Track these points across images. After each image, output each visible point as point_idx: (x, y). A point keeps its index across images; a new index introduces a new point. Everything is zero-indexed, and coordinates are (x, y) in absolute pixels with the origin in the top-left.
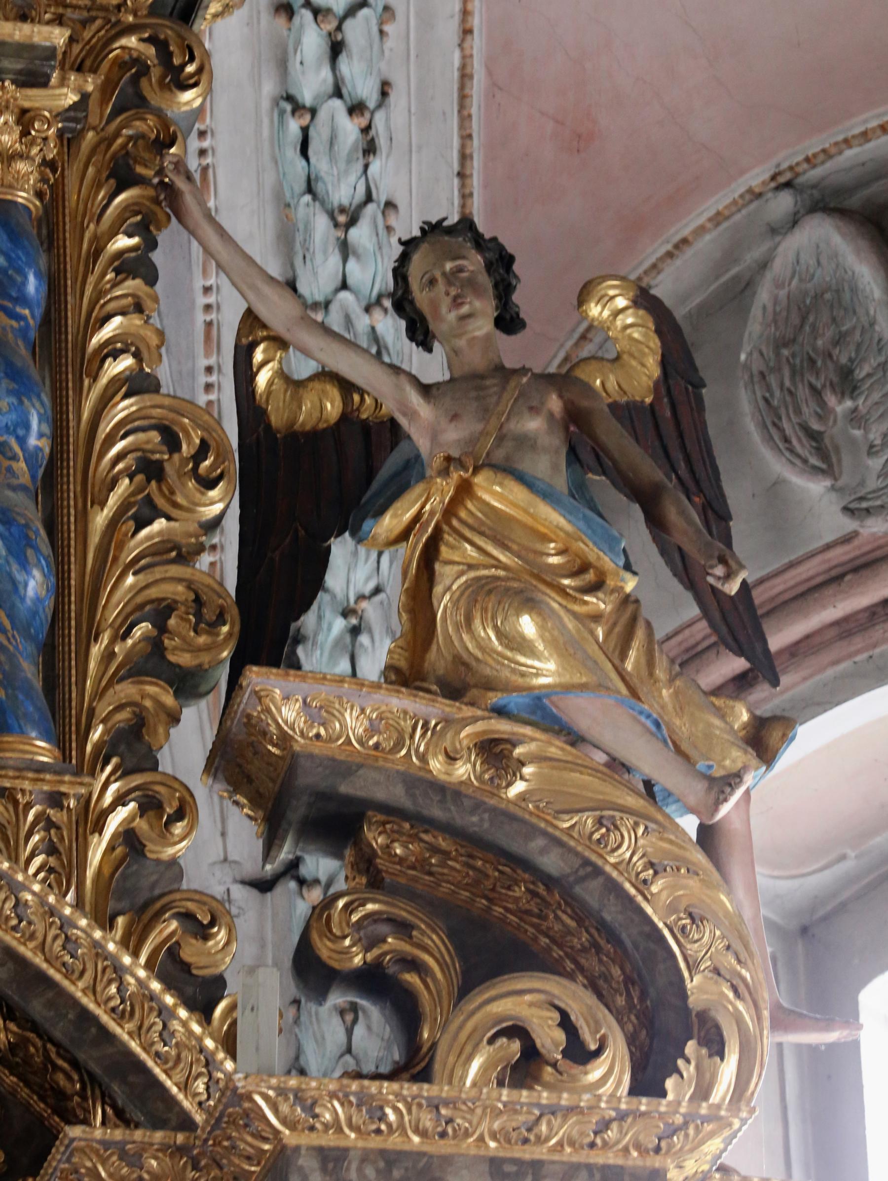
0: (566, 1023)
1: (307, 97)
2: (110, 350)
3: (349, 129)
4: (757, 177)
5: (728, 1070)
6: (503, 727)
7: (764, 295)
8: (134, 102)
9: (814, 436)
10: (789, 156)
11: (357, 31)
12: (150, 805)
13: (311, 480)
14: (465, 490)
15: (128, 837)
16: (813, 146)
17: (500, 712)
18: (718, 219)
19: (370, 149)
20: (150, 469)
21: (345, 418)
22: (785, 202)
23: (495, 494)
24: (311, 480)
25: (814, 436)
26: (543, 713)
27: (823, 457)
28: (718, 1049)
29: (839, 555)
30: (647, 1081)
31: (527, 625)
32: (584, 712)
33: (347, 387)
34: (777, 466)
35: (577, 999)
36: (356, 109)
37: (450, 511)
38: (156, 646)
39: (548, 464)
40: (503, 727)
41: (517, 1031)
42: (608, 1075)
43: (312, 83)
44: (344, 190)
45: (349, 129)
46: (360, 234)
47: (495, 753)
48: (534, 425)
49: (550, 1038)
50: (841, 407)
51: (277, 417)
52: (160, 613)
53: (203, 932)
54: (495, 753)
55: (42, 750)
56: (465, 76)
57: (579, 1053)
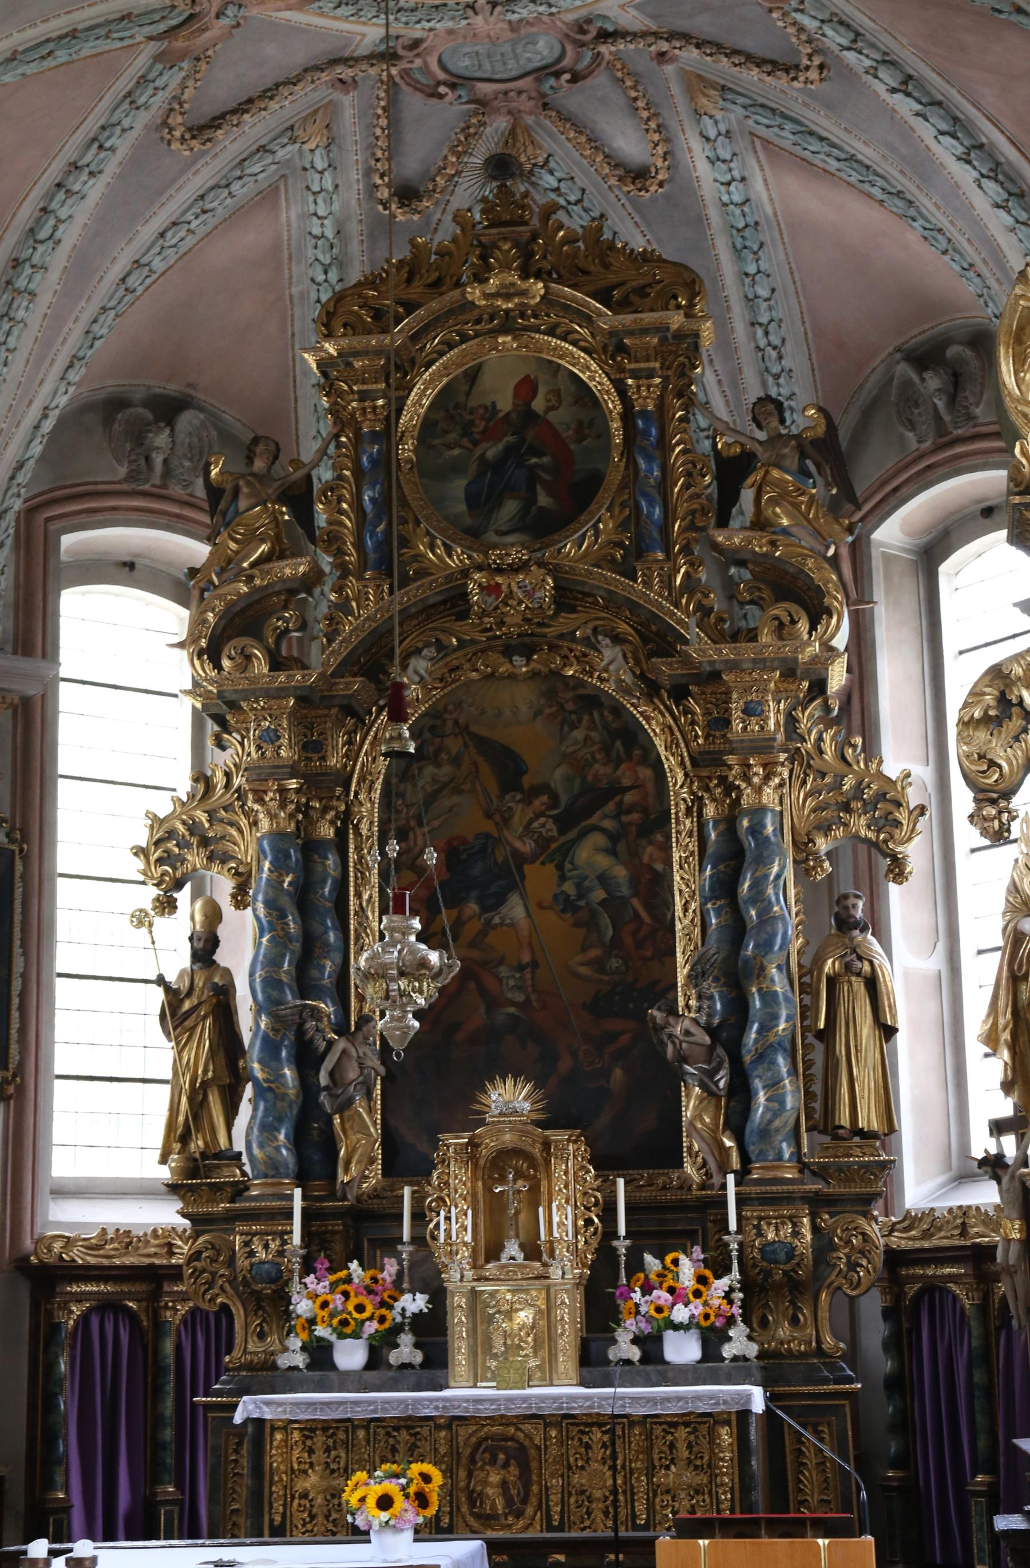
0: (790, 615)
1: (762, 346)
2: (678, 444)
3: (774, 354)
4: (891, 349)
5: (834, 620)
6: (774, 537)
7: (895, 382)
8: (682, 375)
9: (910, 420)
10: (898, 342)
11: (772, 327)
12: (691, 564)
13: (733, 470)
14: (767, 472)
15: (687, 573)
16: (903, 339)
17: (774, 533)
18: (882, 361)
19: (780, 357)
20: (689, 474)
21: (743, 451)
22: (898, 356)
23: (775, 473)
24: (733, 470)
25: (910, 420)
26: (785, 531)
27: (912, 426)
28: (831, 617)
29: (916, 454)
30: (813, 628)
31: (778, 510)
32: (794, 530)
33: (742, 445)
34: (901, 429)
35: (793, 608)
36: (775, 348)
37: (764, 478)
38: (692, 522)
39: (792, 461)
40: (774, 537)
41: (777, 618)
42: (803, 626)
43: (762, 343)
44: (776, 369)
45: (774, 354)
46: (781, 381)
47: (773, 544)
48: (786, 451)
49: (786, 619)
50: (916, 411)
51: (725, 454)
52: (693, 512)
53: (707, 596)
54: (773, 544)
55: (660, 556)
56: (806, 334)
57: (794, 622)
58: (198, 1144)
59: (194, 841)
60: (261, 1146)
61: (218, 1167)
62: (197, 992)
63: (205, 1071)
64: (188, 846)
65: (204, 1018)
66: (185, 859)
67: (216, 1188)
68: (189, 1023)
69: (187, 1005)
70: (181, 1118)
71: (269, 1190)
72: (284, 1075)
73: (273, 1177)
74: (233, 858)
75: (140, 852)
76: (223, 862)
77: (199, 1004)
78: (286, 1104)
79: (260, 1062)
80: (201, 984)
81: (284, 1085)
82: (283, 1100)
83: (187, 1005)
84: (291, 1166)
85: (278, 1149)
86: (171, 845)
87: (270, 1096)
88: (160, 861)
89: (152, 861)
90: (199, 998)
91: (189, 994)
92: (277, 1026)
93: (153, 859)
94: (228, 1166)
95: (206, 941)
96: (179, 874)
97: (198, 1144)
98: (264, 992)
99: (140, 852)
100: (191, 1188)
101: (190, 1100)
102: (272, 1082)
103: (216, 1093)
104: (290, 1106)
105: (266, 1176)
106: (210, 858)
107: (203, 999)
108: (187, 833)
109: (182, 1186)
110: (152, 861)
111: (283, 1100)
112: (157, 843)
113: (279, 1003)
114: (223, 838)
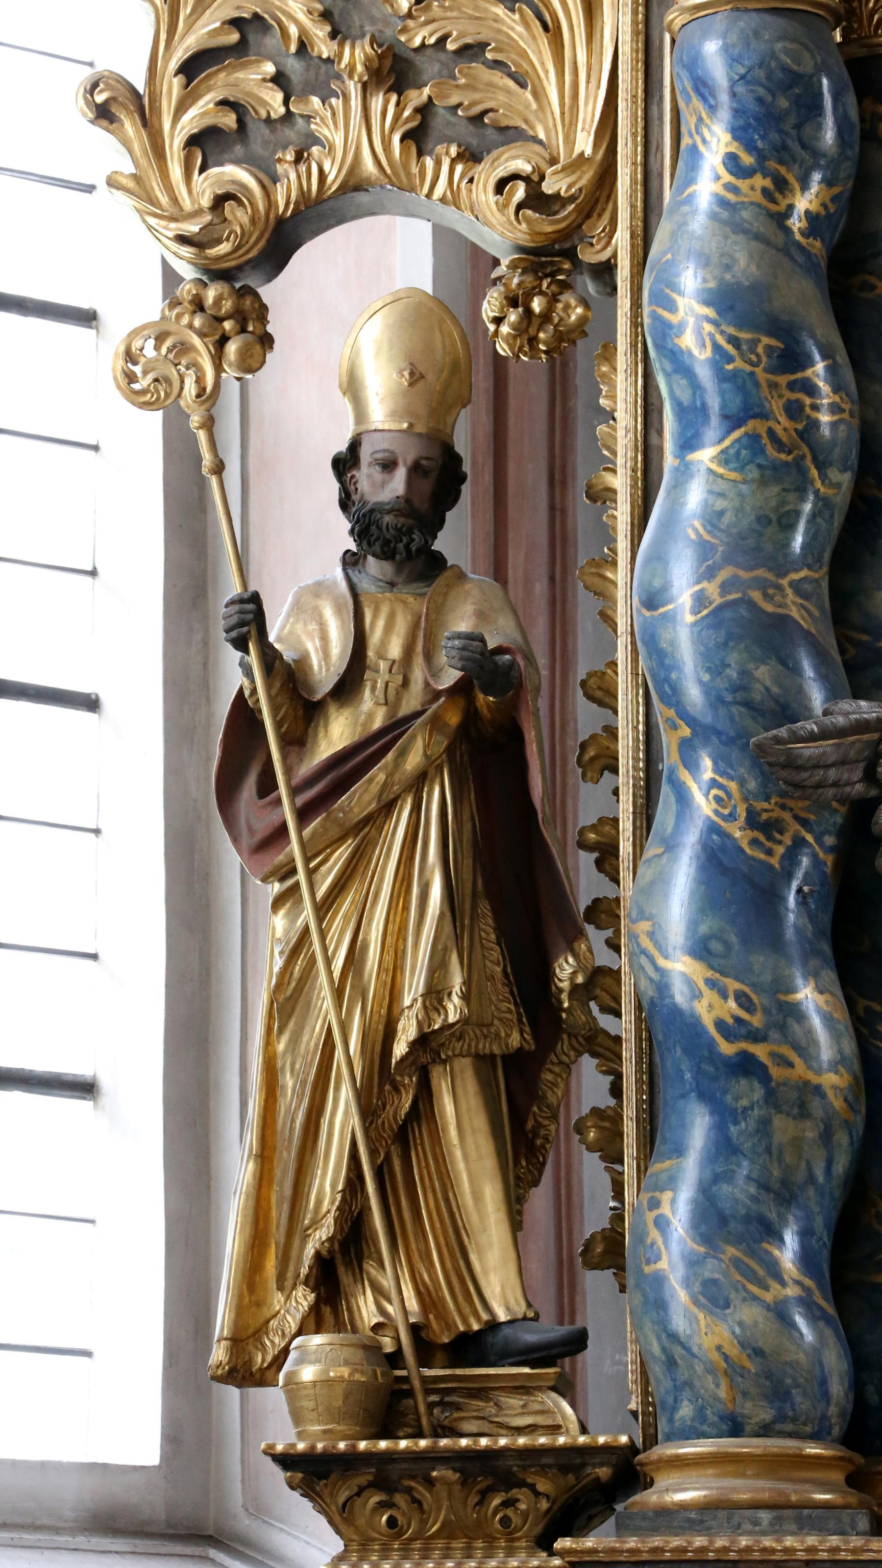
58: (386, 1300)
59: (357, 55)
60: (713, 1297)
61: (481, 1391)
62: (379, 676)
63: (434, 995)
64: (323, 79)
65: (419, 782)
66: (314, 140)
67: (490, 1472)
68: (360, 799)
69: (337, 733)
70: (327, 1183)
71: (744, 1488)
72: (795, 1012)
73: (765, 1431)
74: (511, 135)
75: (112, 105)
76: (471, 156)
77: (395, 730)
78: (811, 1134)
79: (701, 949)
80: (395, 650)
81: (805, 1049)
82: (803, 1112)
83: (337, 733)
84: (838, 1388)
85: (780, 1314)
86: (254, 80)
87: (747, 1093)
88: (206, 144)
89: (175, 145)
90: (390, 702)
91: (348, 687)
92: (768, 808)
93: (176, 134)
94: (523, 1388)
95: (416, 470)
96: (283, 196)
97: (386, 1300)
98: (713, 664)
99: (112, 105)
100: (385, 1474)
101: (369, 1109)
102: (756, 1037)
103: (470, 1085)
104: (826, 1137)
105: (736, 1429)
106: (418, 137)
107: (411, 702)
108: (319, 32)
109: (350, 1462)
110: (175, 145)
111: (803, 1112)
112: (193, 68)
113: (787, 710)
114: (472, 51)
